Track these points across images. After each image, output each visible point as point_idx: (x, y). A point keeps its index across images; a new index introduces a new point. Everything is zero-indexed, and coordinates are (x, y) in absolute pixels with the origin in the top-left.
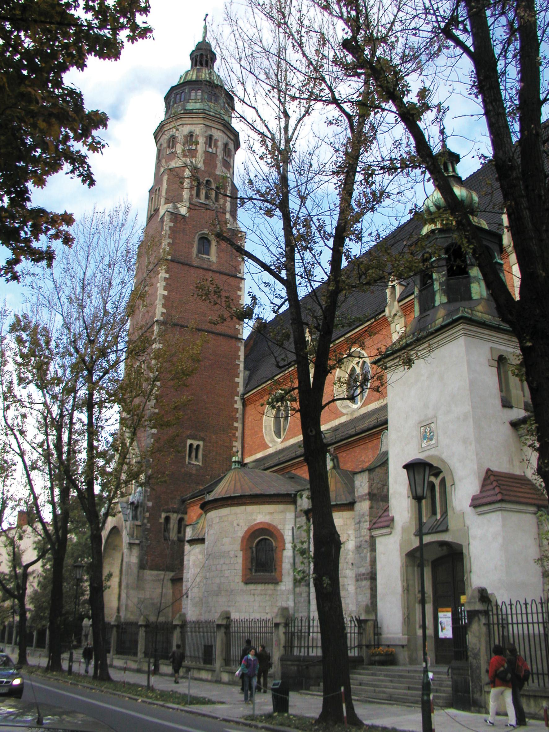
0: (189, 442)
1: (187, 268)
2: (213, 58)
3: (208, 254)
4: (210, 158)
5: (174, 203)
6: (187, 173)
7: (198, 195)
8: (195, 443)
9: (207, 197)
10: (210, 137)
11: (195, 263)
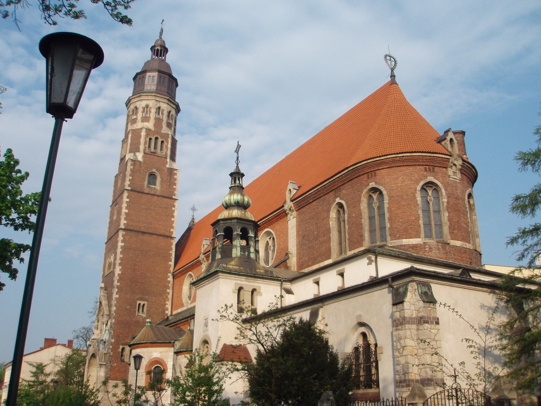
0: (138, 302)
1: (140, 194)
2: (166, 50)
3: (155, 184)
4: (158, 122)
5: (134, 153)
6: (143, 133)
7: (149, 147)
8: (142, 303)
9: (155, 148)
10: (159, 108)
11: (146, 192)
